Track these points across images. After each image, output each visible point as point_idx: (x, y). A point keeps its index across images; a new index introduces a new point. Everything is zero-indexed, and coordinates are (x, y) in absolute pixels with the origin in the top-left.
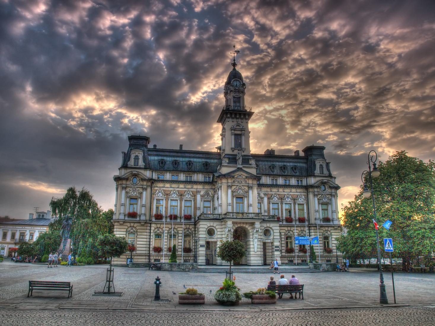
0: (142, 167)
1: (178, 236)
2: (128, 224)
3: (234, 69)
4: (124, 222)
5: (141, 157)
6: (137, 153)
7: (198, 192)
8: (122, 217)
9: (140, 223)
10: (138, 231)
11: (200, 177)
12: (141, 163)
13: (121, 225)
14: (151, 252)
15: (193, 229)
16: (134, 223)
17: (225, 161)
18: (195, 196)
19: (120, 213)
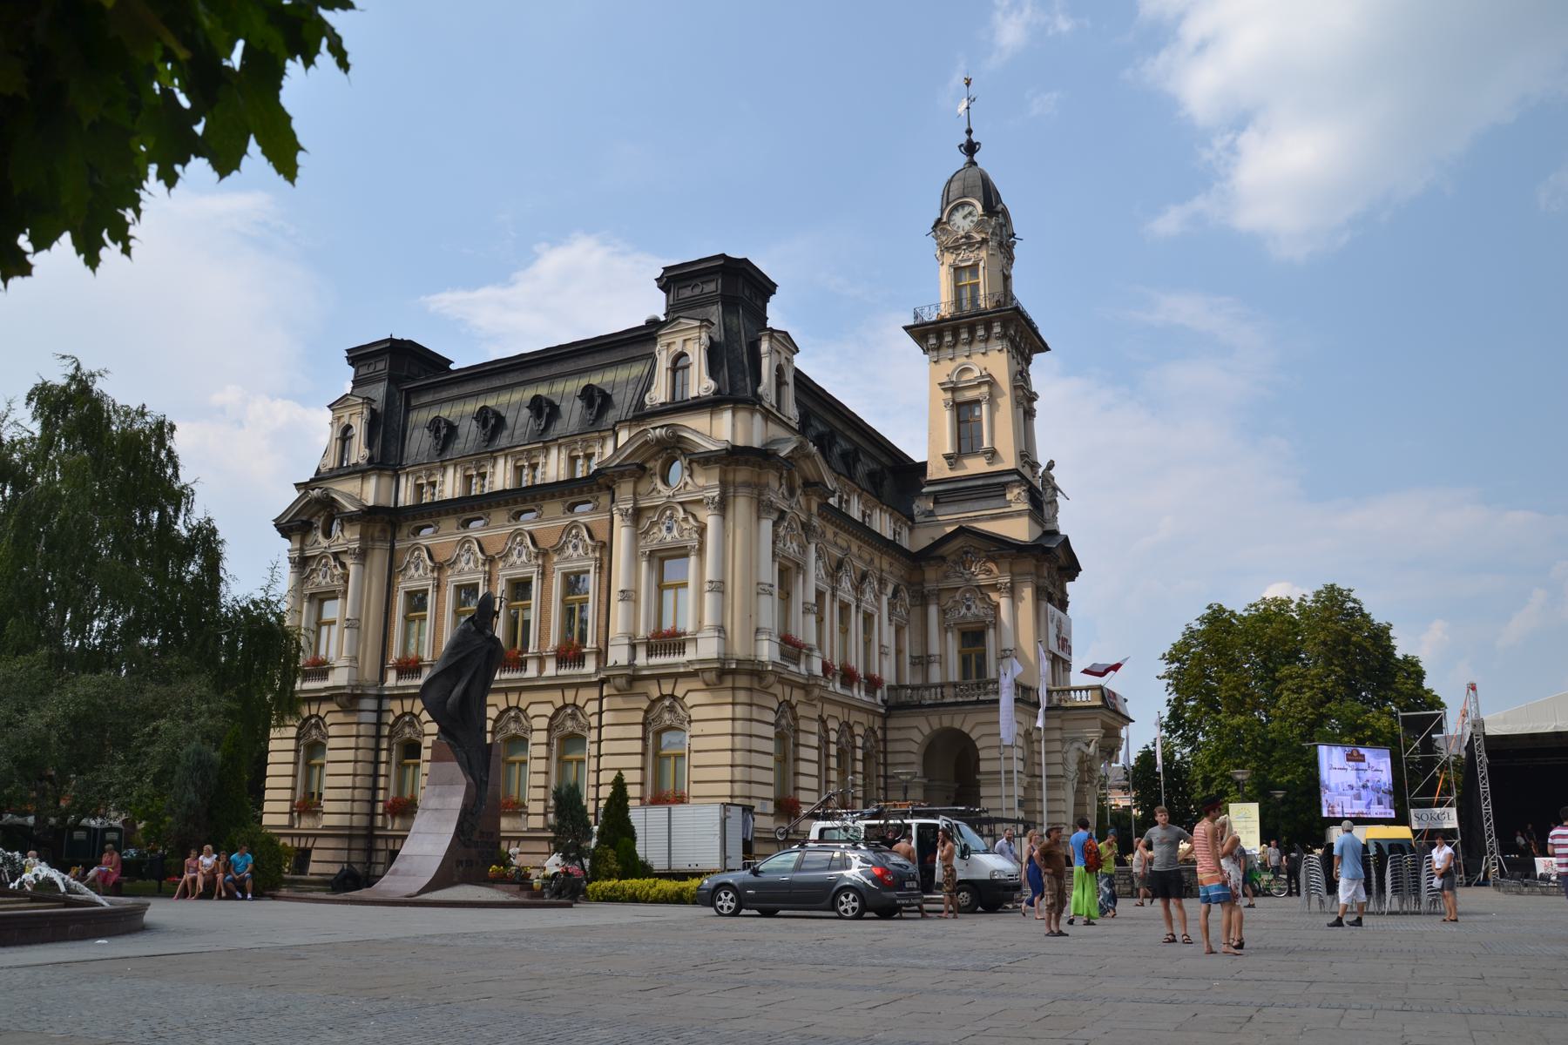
0: (793, 424)
1: (854, 760)
2: (777, 689)
3: (972, 163)
4: (783, 681)
5: (790, 378)
6: (783, 355)
7: (882, 582)
8: (768, 651)
9: (806, 688)
10: (803, 725)
11: (883, 524)
12: (791, 411)
13: (765, 691)
14: (379, 821)
15: (879, 733)
16: (793, 685)
17: (1017, 498)
18: (878, 598)
19: (758, 631)
